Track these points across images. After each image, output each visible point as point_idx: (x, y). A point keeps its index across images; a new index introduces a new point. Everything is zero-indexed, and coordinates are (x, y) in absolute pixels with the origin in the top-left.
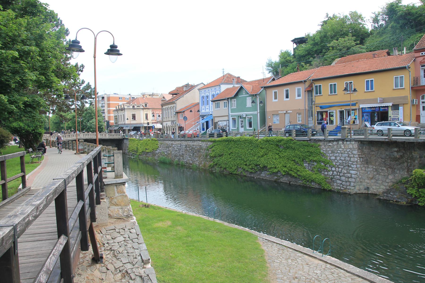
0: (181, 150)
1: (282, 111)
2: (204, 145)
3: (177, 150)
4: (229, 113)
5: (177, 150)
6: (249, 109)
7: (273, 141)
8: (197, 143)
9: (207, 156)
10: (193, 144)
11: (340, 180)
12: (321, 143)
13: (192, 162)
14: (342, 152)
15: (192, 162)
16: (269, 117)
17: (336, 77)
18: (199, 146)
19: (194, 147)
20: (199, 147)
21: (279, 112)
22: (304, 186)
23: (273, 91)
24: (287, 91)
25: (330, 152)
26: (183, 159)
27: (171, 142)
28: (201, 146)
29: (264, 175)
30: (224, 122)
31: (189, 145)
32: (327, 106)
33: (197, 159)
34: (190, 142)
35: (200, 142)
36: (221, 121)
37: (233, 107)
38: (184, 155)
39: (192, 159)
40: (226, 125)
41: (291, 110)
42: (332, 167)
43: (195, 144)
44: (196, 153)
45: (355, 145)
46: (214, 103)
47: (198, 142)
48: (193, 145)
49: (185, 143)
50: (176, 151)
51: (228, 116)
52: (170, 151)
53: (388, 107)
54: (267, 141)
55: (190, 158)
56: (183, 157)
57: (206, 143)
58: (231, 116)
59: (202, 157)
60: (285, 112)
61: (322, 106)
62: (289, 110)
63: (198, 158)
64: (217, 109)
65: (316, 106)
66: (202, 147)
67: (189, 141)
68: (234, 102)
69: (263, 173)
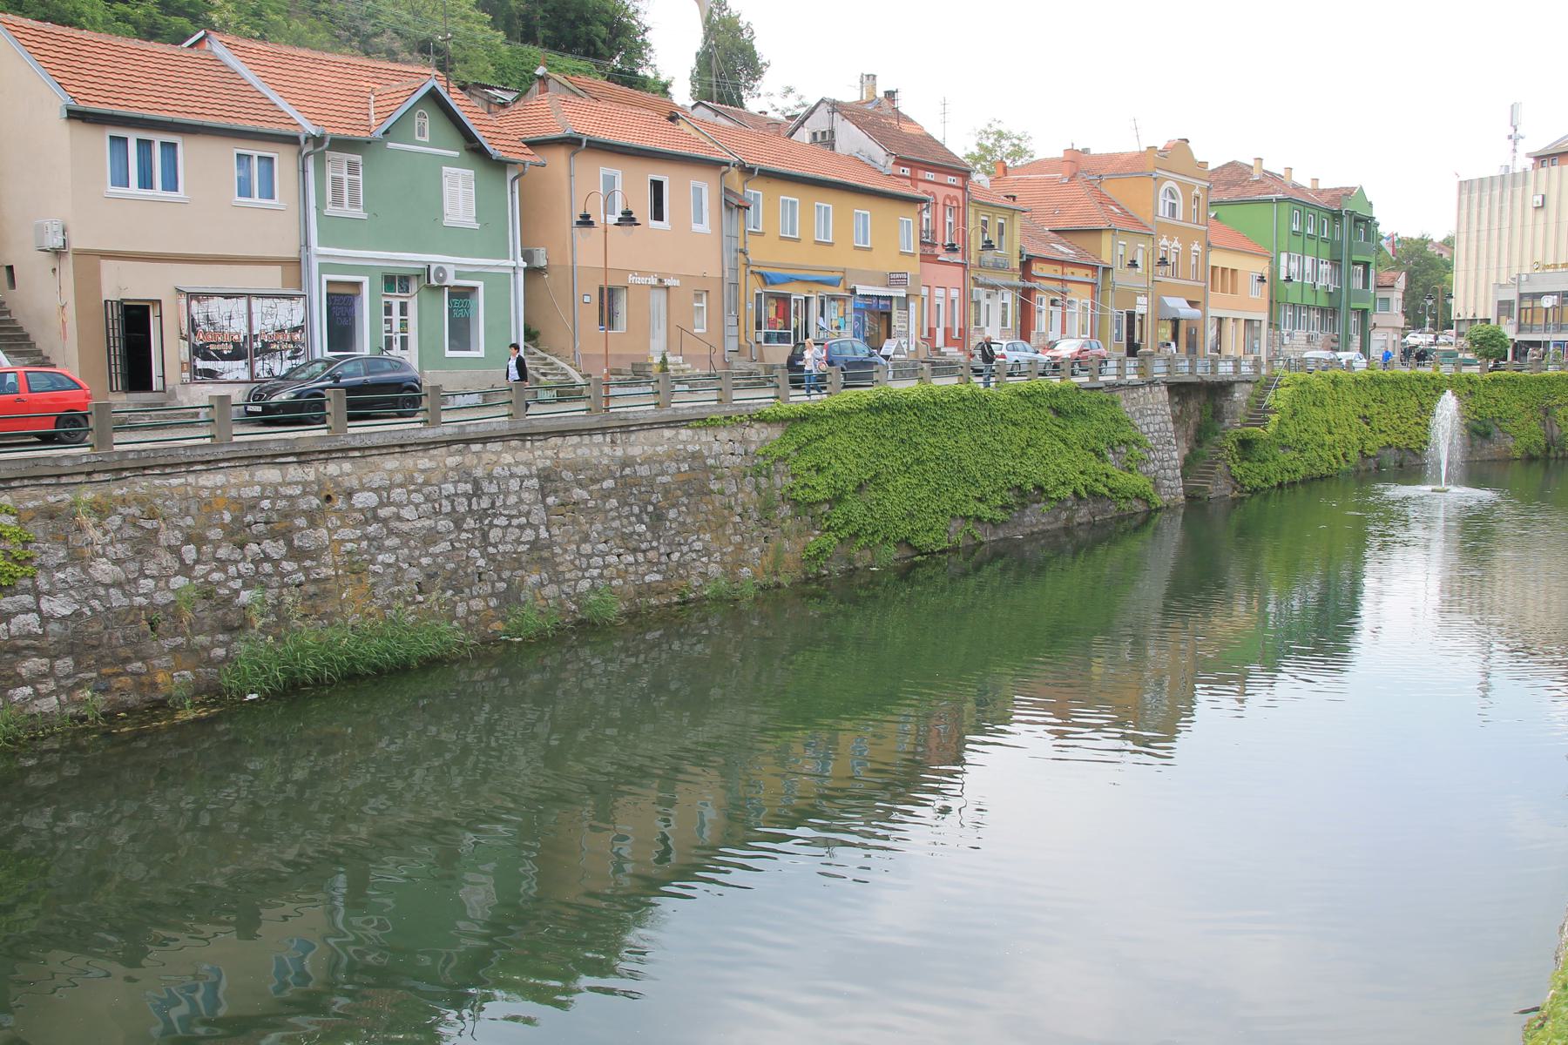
0: (503, 521)
1: (641, 273)
2: (715, 444)
3: (444, 524)
4: (307, 245)
5: (444, 524)
6: (458, 240)
7: (1042, 394)
8: (654, 445)
9: (767, 508)
10: (619, 452)
11: (1165, 478)
12: (1119, 394)
13: (658, 577)
14: (1154, 412)
15: (658, 577)
16: (587, 299)
17: (771, 172)
18: (685, 459)
19: (643, 471)
20: (685, 467)
21: (631, 279)
22: (1119, 516)
23: (604, 171)
24: (657, 187)
25: (1138, 415)
26: (559, 583)
27: (310, 473)
28: (694, 456)
29: (1037, 517)
30: (268, 302)
31: (576, 469)
32: (783, 276)
33: (698, 545)
34: (575, 446)
35: (685, 434)
36: (228, 296)
37: (337, 202)
38: (549, 547)
39: (651, 554)
40: (295, 330)
41: (676, 277)
42: (1148, 452)
43: (635, 451)
44: (674, 506)
45: (1162, 394)
46: (100, 138)
47: (668, 433)
48: (626, 462)
49: (523, 456)
50: (431, 537)
51: (295, 266)
52: (328, 558)
53: (890, 298)
54: (1026, 397)
55: (635, 551)
56: (548, 563)
57: (736, 434)
58: (324, 268)
59: (738, 519)
60: (654, 281)
61: (773, 274)
62: (668, 276)
63: (708, 537)
64: (158, 191)
65: (752, 272)
66: (710, 462)
67: (576, 439)
68: (345, 176)
69: (1028, 512)
